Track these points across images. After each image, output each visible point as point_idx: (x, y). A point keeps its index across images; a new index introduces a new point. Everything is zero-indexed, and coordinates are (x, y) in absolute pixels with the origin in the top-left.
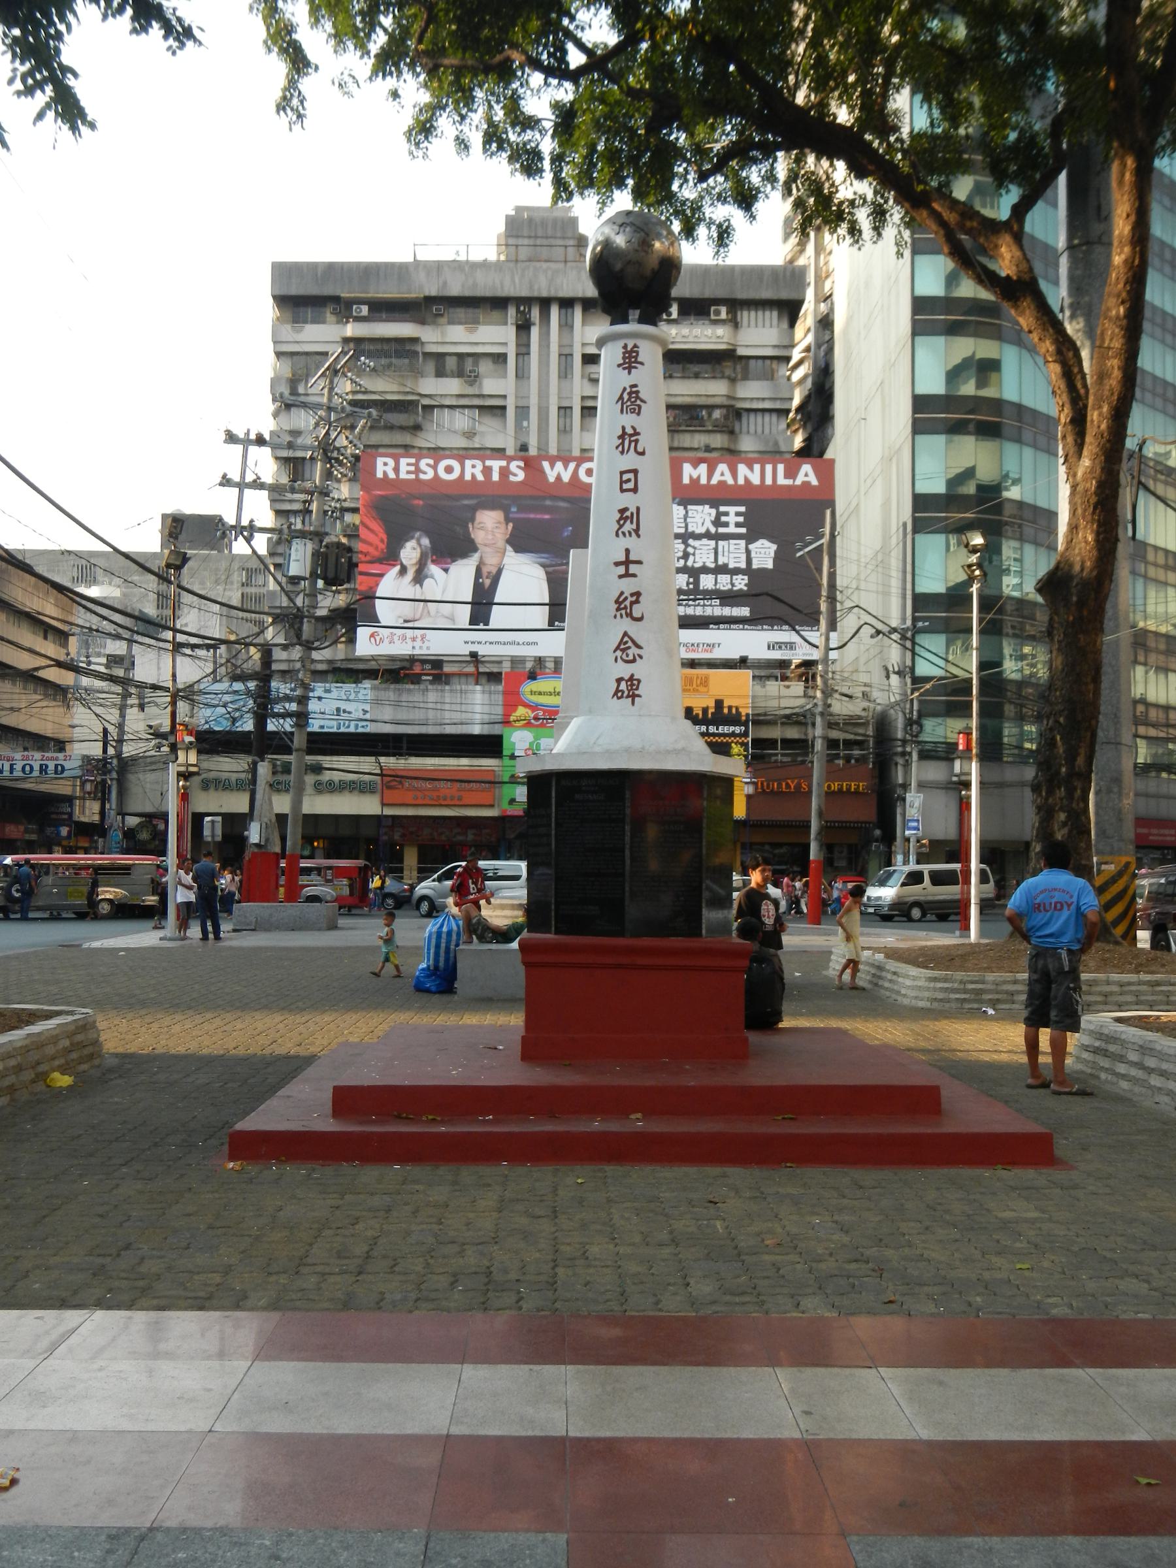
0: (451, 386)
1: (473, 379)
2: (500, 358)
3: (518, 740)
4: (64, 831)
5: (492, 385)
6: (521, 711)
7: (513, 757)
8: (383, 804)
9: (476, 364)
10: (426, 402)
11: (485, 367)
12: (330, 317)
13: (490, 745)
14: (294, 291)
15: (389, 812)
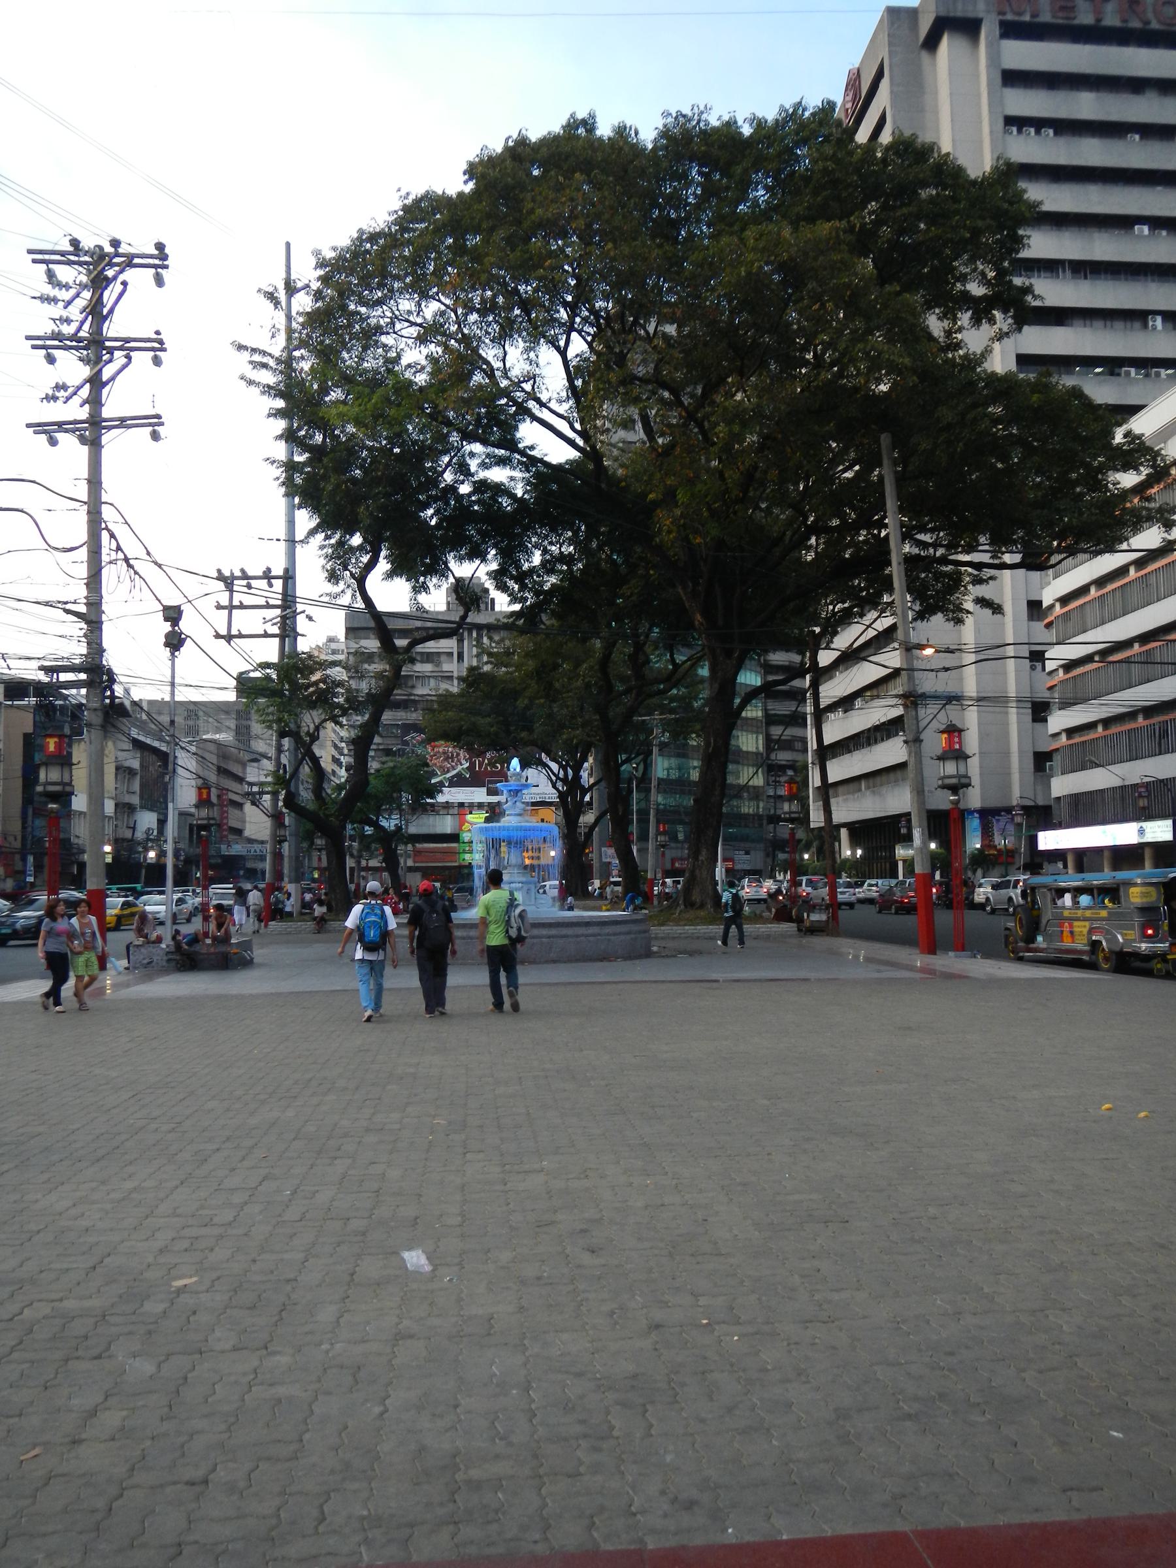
0: (427, 668)
1: (438, 664)
2: (451, 654)
3: (466, 836)
4: (242, 873)
5: (446, 667)
6: (466, 826)
7: (464, 843)
8: (415, 862)
9: (439, 657)
10: (416, 674)
11: (443, 658)
12: (372, 636)
13: (454, 838)
14: (356, 626)
15: (417, 865)
